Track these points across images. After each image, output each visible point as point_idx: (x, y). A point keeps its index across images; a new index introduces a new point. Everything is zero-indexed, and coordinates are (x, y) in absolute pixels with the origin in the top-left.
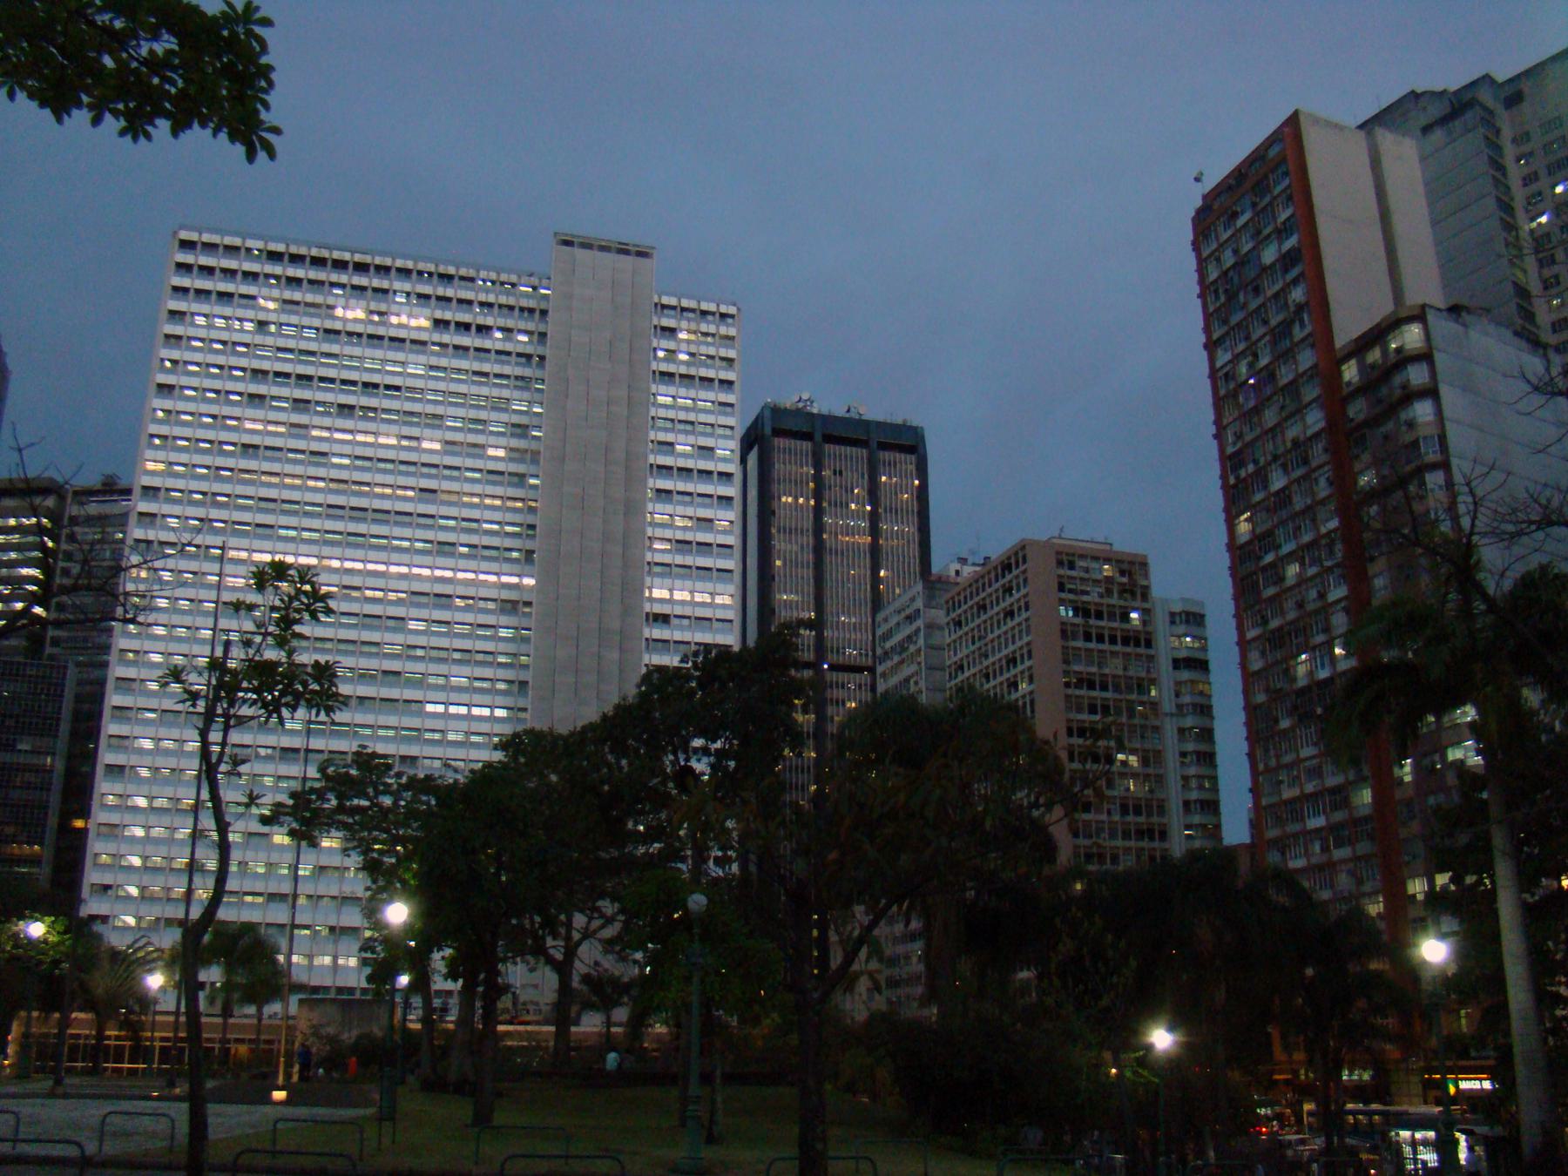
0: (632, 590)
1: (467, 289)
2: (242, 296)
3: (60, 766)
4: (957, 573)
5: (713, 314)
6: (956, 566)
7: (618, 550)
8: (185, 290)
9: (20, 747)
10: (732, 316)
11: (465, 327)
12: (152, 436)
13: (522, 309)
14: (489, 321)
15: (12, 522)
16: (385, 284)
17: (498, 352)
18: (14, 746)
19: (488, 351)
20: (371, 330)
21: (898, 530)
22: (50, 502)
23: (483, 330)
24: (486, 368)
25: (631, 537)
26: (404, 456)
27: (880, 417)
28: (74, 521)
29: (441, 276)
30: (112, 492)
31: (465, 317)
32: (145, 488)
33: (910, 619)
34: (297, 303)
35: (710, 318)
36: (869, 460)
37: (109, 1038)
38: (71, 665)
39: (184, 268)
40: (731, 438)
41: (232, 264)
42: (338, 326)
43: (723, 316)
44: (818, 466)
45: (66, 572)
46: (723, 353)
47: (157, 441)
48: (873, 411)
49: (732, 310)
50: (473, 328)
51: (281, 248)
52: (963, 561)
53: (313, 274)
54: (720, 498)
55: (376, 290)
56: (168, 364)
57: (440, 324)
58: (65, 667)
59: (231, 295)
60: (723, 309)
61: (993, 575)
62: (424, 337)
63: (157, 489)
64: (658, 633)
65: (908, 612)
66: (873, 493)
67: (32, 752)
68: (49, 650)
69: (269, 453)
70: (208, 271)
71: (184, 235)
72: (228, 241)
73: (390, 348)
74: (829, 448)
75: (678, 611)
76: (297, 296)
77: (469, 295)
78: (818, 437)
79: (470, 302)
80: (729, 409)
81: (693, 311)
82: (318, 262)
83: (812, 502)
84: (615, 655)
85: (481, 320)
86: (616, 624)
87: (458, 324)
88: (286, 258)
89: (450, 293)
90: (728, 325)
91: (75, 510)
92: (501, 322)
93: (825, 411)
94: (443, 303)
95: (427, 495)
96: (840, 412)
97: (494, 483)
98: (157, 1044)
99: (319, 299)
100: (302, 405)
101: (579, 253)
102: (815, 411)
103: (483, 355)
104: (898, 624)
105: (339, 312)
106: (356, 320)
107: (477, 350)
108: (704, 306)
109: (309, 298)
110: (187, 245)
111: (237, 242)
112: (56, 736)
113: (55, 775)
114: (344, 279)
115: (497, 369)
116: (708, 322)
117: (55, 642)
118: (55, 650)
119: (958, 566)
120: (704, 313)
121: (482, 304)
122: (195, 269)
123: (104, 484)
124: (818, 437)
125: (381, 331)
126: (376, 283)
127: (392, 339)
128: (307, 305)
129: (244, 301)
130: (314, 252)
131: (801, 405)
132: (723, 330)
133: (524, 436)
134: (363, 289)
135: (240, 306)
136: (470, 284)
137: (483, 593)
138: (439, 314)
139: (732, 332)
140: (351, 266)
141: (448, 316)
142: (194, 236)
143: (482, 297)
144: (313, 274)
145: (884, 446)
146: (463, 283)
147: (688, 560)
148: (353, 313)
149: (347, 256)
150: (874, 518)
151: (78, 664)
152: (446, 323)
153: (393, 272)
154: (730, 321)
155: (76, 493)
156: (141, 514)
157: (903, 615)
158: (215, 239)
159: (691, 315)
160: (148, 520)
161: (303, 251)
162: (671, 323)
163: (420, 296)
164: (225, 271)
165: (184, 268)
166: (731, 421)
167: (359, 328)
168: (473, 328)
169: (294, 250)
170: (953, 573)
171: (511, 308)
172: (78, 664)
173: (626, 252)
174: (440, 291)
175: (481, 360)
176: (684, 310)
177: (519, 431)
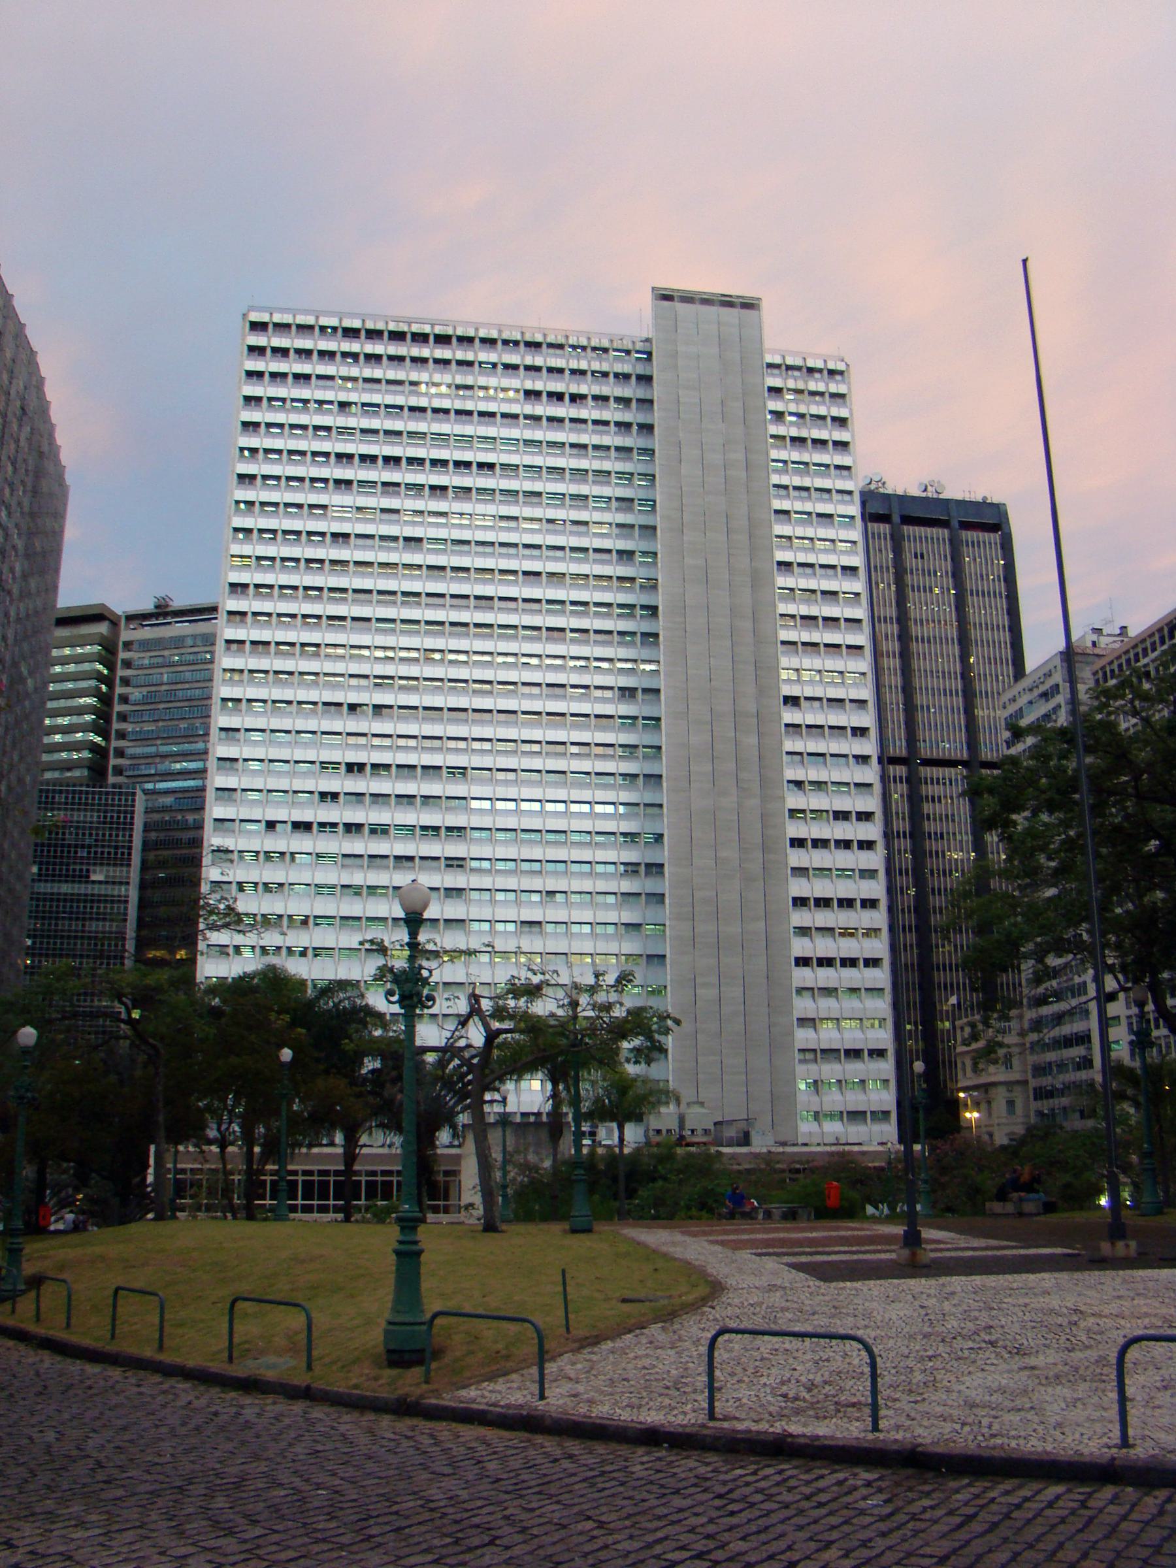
0: (765, 671)
1: (556, 356)
2: (319, 377)
3: (133, 894)
4: (1094, 644)
5: (820, 371)
6: (1094, 637)
7: (749, 625)
8: (260, 375)
9: (94, 878)
10: (841, 373)
11: (559, 397)
12: (236, 530)
13: (616, 375)
14: (583, 389)
15: (67, 651)
16: (470, 356)
17: (595, 422)
18: (88, 877)
19: (584, 421)
20: (458, 405)
21: (985, 613)
22: (103, 628)
23: (575, 398)
24: (584, 439)
25: (761, 612)
26: (505, 537)
27: (958, 496)
28: (128, 645)
29: (529, 344)
30: (166, 615)
31: (557, 386)
32: (231, 585)
33: (1045, 696)
34: (378, 381)
35: (817, 375)
36: (951, 541)
37: (358, 1173)
38: (138, 791)
39: (256, 351)
40: (852, 502)
41: (307, 344)
42: (423, 402)
43: (832, 373)
44: (898, 550)
45: (124, 699)
46: (835, 412)
47: (241, 536)
48: (959, 488)
49: (841, 366)
50: (567, 398)
51: (357, 324)
52: (1098, 631)
53: (394, 349)
54: (845, 568)
55: (460, 363)
56: (246, 453)
57: (532, 395)
58: (134, 794)
59: (307, 377)
60: (831, 366)
61: (1157, 638)
62: (515, 409)
63: (246, 586)
64: (790, 716)
65: (1042, 689)
66: (957, 574)
67: (107, 883)
68: (111, 779)
69: (360, 542)
70: (283, 352)
71: (254, 317)
72: (301, 319)
73: (479, 423)
74: (908, 530)
75: (809, 692)
76: (378, 373)
77: (559, 363)
78: (896, 518)
79: (560, 371)
80: (845, 473)
81: (799, 368)
82: (397, 336)
83: (893, 588)
84: (753, 740)
85: (574, 389)
86: (752, 708)
87: (551, 395)
88: (363, 333)
89: (539, 361)
90: (837, 382)
91: (125, 635)
92: (596, 390)
93: (900, 492)
94: (533, 373)
95: (483, 603)
96: (915, 492)
97: (602, 562)
98: (300, 1178)
99: (400, 375)
100: (391, 489)
101: (679, 306)
102: (890, 491)
103: (579, 426)
104: (1031, 702)
105: (423, 388)
106: (440, 395)
107: (572, 420)
108: (810, 364)
109: (391, 375)
110: (258, 327)
111: (311, 320)
112: (129, 865)
113: (130, 906)
114: (425, 352)
115: (596, 440)
116: (817, 381)
117: (119, 771)
118: (120, 779)
119: (1094, 637)
120: (811, 370)
121: (573, 372)
122: (269, 351)
123: (157, 607)
124: (896, 518)
125: (469, 406)
126: (460, 355)
127: (482, 414)
128: (389, 382)
129: (322, 383)
130: (392, 327)
131: (873, 487)
132: (833, 388)
133: (630, 510)
134: (446, 362)
135: (317, 387)
136: (558, 352)
137: (600, 680)
138: (529, 385)
139: (842, 389)
140: (432, 338)
141: (539, 386)
142: (265, 318)
143: (574, 365)
144: (394, 349)
145: (966, 526)
146: (551, 351)
147: (815, 637)
148: (436, 388)
149: (427, 329)
150: (960, 605)
151: (146, 792)
152: (537, 394)
153: (477, 341)
154: (838, 378)
155: (130, 618)
156: (230, 613)
157: (1036, 692)
158: (287, 319)
159: (796, 373)
160: (238, 618)
161: (380, 326)
162: (776, 382)
163: (507, 366)
164: (299, 352)
165: (256, 351)
166: (848, 485)
167: (446, 404)
168: (567, 398)
169: (370, 325)
170: (1089, 644)
171: (605, 375)
172: (146, 792)
173: (730, 304)
174: (529, 361)
175: (579, 431)
176: (789, 368)
177: (624, 504)
